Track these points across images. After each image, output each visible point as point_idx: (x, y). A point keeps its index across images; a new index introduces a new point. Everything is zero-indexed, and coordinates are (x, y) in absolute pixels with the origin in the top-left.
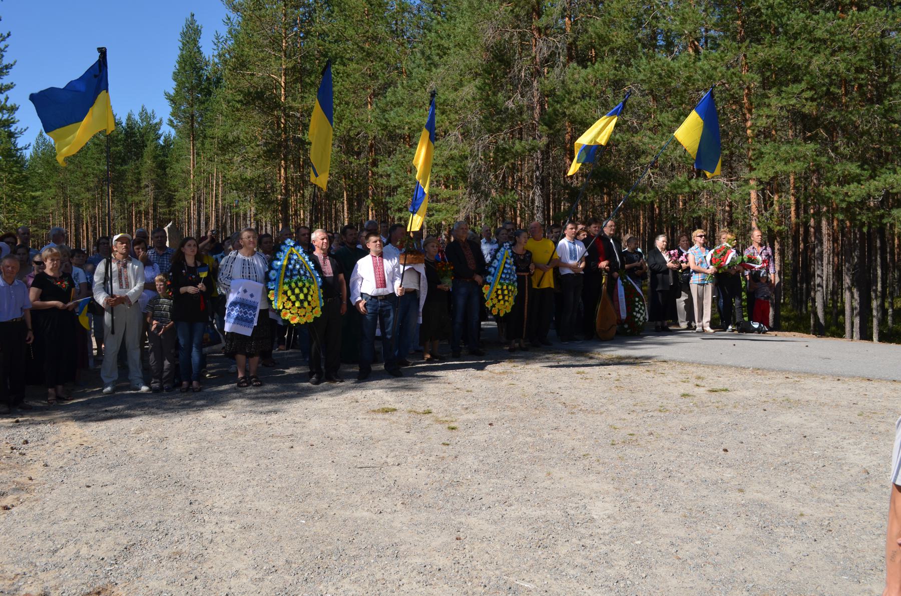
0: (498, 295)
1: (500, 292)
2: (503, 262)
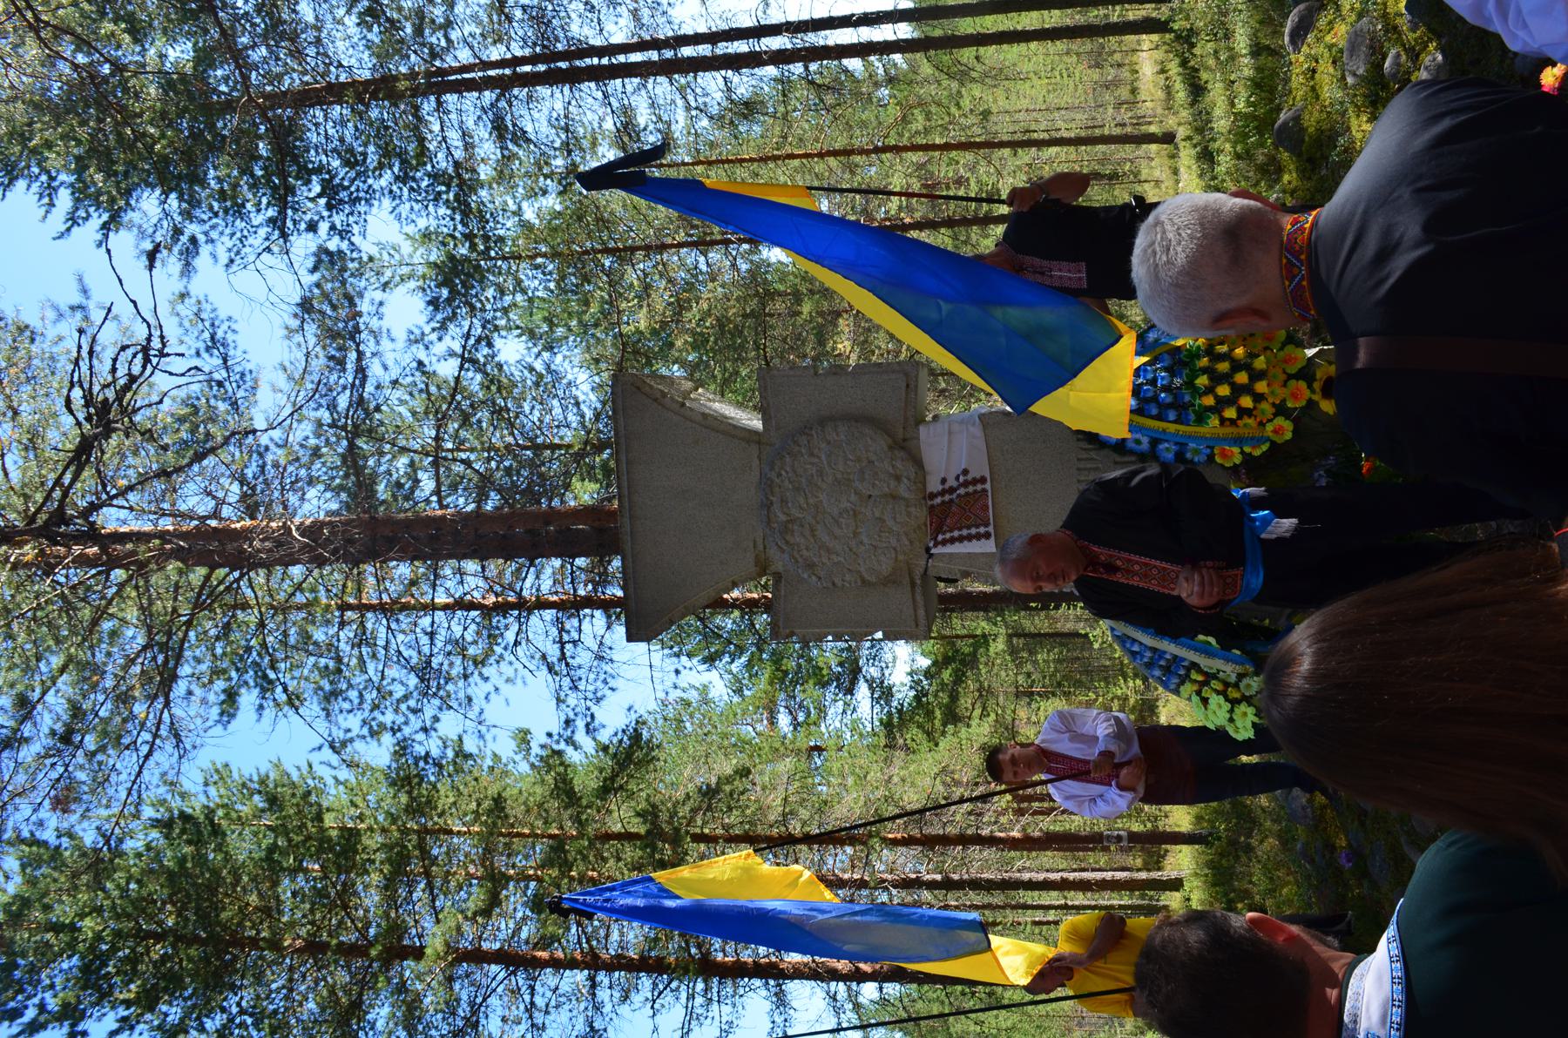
0: (1243, 412)
1: (1231, 413)
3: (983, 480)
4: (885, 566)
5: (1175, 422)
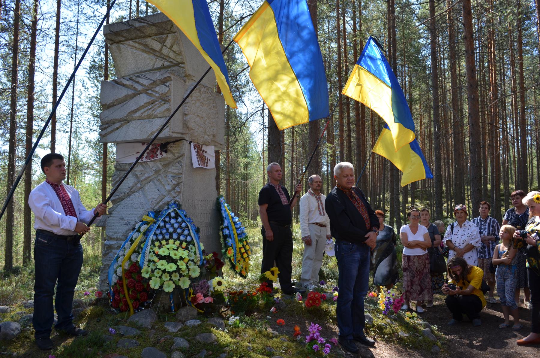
2: (230, 218)
3: (207, 166)
4: (191, 125)
5: (238, 234)
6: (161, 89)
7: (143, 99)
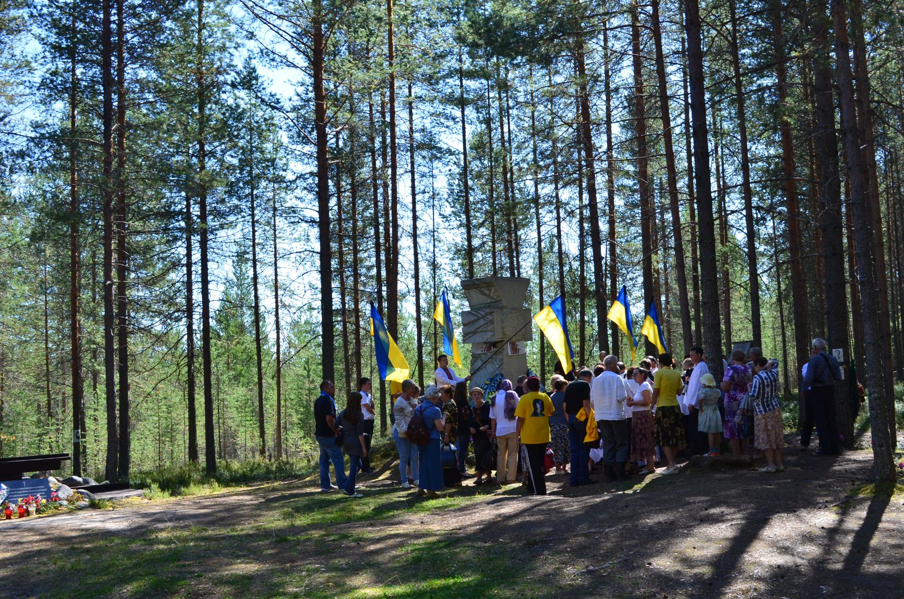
6: (489, 317)
7: (482, 322)
